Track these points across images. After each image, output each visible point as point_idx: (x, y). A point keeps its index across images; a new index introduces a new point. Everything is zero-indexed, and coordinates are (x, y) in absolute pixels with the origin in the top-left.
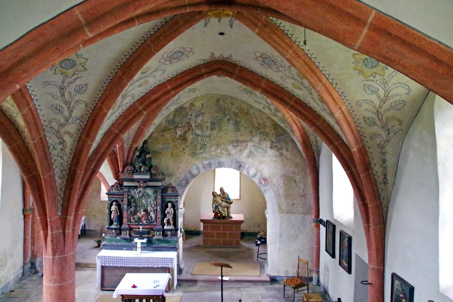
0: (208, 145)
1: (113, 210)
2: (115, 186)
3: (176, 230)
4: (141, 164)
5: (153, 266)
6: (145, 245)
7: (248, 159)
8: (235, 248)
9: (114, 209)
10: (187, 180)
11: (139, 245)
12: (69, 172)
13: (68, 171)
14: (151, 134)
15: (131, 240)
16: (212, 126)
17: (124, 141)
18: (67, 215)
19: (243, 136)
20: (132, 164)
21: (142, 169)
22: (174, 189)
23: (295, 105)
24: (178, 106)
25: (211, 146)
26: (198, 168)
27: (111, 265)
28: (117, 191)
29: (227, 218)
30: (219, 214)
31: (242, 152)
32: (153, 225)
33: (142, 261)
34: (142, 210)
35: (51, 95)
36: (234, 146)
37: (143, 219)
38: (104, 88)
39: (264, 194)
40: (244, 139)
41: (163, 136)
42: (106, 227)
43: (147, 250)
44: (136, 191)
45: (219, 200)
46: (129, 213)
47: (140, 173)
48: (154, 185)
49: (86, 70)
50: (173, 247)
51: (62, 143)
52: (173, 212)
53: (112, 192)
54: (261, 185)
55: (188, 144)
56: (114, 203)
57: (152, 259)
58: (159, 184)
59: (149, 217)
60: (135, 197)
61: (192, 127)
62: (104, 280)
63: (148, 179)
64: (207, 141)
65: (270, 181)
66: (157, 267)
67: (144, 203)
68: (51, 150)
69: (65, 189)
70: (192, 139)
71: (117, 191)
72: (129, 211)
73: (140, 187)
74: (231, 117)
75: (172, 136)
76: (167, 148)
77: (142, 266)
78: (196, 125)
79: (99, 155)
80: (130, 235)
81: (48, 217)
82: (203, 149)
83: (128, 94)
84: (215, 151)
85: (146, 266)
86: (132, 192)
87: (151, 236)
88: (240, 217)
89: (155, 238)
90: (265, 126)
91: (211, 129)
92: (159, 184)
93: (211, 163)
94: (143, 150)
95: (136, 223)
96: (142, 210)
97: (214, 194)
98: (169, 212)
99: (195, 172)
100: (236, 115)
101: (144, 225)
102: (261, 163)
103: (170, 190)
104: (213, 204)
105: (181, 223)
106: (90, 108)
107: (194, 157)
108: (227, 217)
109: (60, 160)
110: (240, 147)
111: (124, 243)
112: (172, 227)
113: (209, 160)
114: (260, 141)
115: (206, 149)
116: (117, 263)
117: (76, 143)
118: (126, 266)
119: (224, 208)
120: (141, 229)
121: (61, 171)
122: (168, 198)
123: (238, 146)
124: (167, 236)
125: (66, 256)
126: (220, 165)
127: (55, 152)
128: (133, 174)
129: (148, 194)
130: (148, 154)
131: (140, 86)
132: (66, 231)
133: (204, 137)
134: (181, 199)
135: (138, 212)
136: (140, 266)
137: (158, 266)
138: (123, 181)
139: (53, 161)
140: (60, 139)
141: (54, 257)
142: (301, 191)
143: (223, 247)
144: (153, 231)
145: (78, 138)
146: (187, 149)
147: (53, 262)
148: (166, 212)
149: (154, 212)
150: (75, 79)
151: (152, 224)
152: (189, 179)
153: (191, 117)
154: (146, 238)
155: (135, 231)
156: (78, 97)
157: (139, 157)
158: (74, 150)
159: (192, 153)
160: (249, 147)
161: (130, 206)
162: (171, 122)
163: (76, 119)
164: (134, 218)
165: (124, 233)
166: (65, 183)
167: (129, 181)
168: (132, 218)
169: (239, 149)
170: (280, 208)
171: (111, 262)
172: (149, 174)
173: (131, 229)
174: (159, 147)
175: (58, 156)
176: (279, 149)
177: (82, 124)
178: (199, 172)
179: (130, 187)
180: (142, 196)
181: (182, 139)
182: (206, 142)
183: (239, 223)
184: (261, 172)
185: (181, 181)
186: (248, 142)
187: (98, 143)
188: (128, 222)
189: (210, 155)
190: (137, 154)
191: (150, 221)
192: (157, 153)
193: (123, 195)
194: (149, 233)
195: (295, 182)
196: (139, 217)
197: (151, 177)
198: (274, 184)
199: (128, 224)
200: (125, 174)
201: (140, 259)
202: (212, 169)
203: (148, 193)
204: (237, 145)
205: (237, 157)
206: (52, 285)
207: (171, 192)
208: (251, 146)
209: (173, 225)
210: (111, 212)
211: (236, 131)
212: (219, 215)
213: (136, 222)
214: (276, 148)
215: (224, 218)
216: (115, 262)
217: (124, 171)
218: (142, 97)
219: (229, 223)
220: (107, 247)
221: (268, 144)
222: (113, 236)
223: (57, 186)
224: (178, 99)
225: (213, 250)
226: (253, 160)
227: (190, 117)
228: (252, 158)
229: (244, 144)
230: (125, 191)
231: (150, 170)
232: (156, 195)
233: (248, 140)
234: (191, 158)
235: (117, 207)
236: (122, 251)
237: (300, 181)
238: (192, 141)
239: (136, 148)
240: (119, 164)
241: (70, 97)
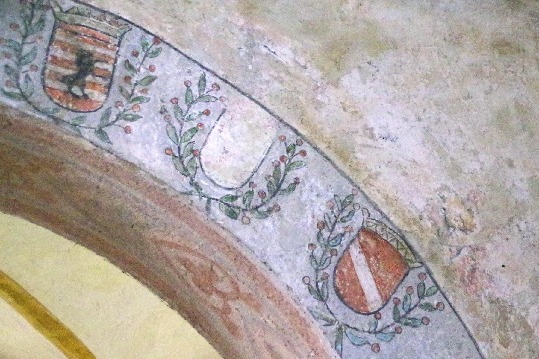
65: (448, 272)
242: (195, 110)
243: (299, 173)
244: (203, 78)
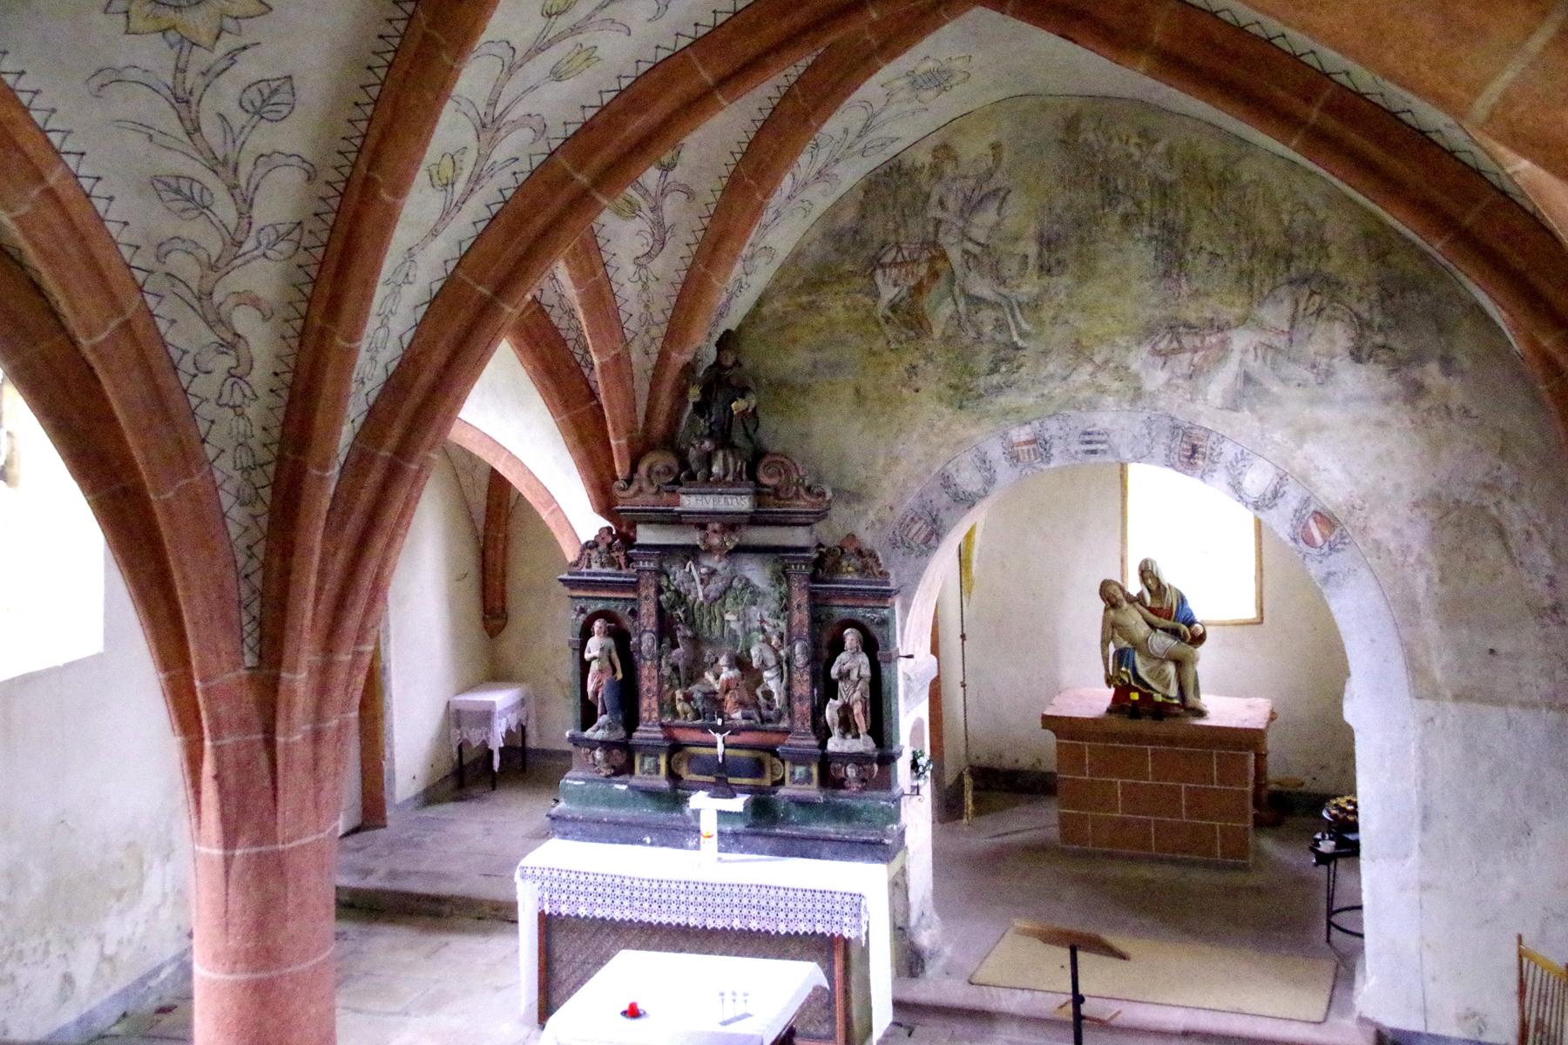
0: (1030, 346)
1: (595, 658)
2: (602, 547)
3: (887, 759)
4: (707, 444)
5: (771, 927)
6: (740, 827)
7: (1235, 414)
8: (1219, 867)
9: (596, 653)
10: (934, 521)
11: (709, 824)
12: (277, 471)
13: (271, 469)
14: (760, 303)
15: (675, 797)
16: (1046, 253)
17: (629, 336)
18: (278, 663)
19: (1203, 300)
20: (669, 442)
21: (716, 469)
22: (870, 561)
23: (1332, 124)
24: (876, 160)
25: (1045, 353)
26: (984, 462)
27: (582, 912)
29: (1177, 715)
30: (1136, 690)
31: (1201, 381)
32: (777, 731)
33: (718, 900)
34: (723, 661)
35: (144, 129)
36: (1156, 352)
37: (730, 700)
38: (375, 91)
39: (1326, 591)
40: (1208, 314)
41: (812, 307)
42: (567, 734)
43: (748, 849)
44: (697, 569)
45: (1135, 621)
46: (667, 671)
47: (710, 484)
48: (776, 543)
49: (271, 9)
50: (865, 842)
51: (233, 346)
52: (866, 672)
53: (589, 574)
54: (1305, 548)
55: (933, 343)
56: (597, 624)
57: (764, 891)
58: (798, 537)
59: (759, 692)
60: (690, 598)
61: (946, 260)
62: (554, 982)
63: (742, 513)
64: (1026, 327)
66: (788, 933)
67: (734, 626)
68: (185, 380)
69: (269, 552)
70: (952, 317)
71: (608, 570)
72: (663, 663)
73: (710, 551)
74: (1138, 204)
75: (856, 310)
76: (836, 367)
77: (720, 924)
78: (966, 252)
79: (415, 398)
80: (673, 776)
81: (196, 675)
82: (1003, 369)
83: (509, 117)
84: (1065, 379)
85: (737, 924)
86: (681, 574)
87: (767, 782)
88: (1247, 714)
89: (782, 791)
90: (1323, 244)
91: (1041, 267)
92: (798, 537)
93: (1047, 437)
94: (718, 377)
95: (699, 722)
96: (723, 661)
97: (1110, 595)
98: (849, 671)
99: (968, 479)
100: (1163, 191)
101: (736, 731)
102: (1301, 434)
103: (850, 569)
104: (1104, 644)
105: (917, 729)
106: (328, 183)
107: (960, 408)
108: (1176, 710)
109: (234, 423)
110: (1188, 355)
111: (647, 811)
112: (863, 744)
113: (1036, 424)
114: (1293, 320)
115: (1019, 367)
116: (608, 901)
117: (295, 343)
118: (645, 917)
119: (1163, 661)
120: (720, 749)
121: (244, 470)
122: (840, 602)
123: (1181, 349)
124: (844, 787)
125: (280, 847)
126: (1093, 447)
127: (203, 387)
128: (674, 492)
129: (747, 583)
130: (743, 396)
131: (557, 75)
132: (280, 739)
133: (1007, 310)
134: (906, 608)
135: (705, 667)
136: (710, 924)
137: (791, 925)
138: (632, 526)
139: (203, 427)
140: (220, 329)
141: (230, 853)
142: (1539, 586)
143: (1161, 861)
144: (776, 761)
145: (299, 323)
146: (930, 367)
147: (227, 873)
148: (834, 672)
149: (782, 668)
150: (232, 56)
151: (770, 726)
153: (938, 213)
154: (744, 792)
155: (692, 757)
156: (264, 138)
157: (700, 409)
158: (288, 378)
159: (951, 386)
160: (1235, 357)
161: (667, 640)
162: (847, 238)
163: (273, 237)
164: (688, 698)
165: (646, 767)
166: (263, 521)
167: (662, 523)
168: (679, 694)
169: (1186, 363)
170: (1416, 670)
171: (582, 899)
172: (748, 490)
173: (675, 747)
174: (797, 360)
175: (222, 401)
176: (1397, 366)
177: (302, 257)
178: (990, 482)
179: (666, 551)
180: (723, 594)
181: (905, 323)
183: (1244, 741)
184: (1304, 479)
185: (905, 525)
187: (405, 346)
188: (662, 713)
189: (1043, 395)
190: (694, 394)
191: (762, 714)
192: (783, 390)
193: (634, 586)
194: (757, 769)
195: (1501, 533)
196: (711, 693)
197: (759, 506)
198: (1378, 544)
199: (662, 725)
200: (640, 490)
201: (709, 889)
202: (1052, 465)
203: (747, 580)
204: (1175, 345)
205: (1177, 405)
206: (223, 976)
207: (856, 577)
208: (1244, 352)
209: (869, 733)
210: (585, 666)
211: (1166, 274)
212: (1135, 696)
213: (698, 715)
214: (1384, 357)
215: (1161, 711)
216: (600, 900)
217: (636, 476)
218: (585, 124)
219: (1184, 741)
220: (569, 827)
221: (1341, 336)
222: (595, 776)
223: (233, 537)
224: (866, 127)
225: (1115, 870)
226: (1261, 419)
227: (935, 212)
228: (1252, 410)
229: (1214, 339)
230: (644, 570)
231: (752, 474)
232: (784, 588)
233: (1233, 323)
234: (947, 411)
235: (610, 642)
236: (638, 848)
237: (1528, 533)
238: (949, 332)
239: (689, 369)
240: (613, 442)
241: (229, 137)
242: (1240, 465)
243: (1285, 488)
244: (1242, 452)
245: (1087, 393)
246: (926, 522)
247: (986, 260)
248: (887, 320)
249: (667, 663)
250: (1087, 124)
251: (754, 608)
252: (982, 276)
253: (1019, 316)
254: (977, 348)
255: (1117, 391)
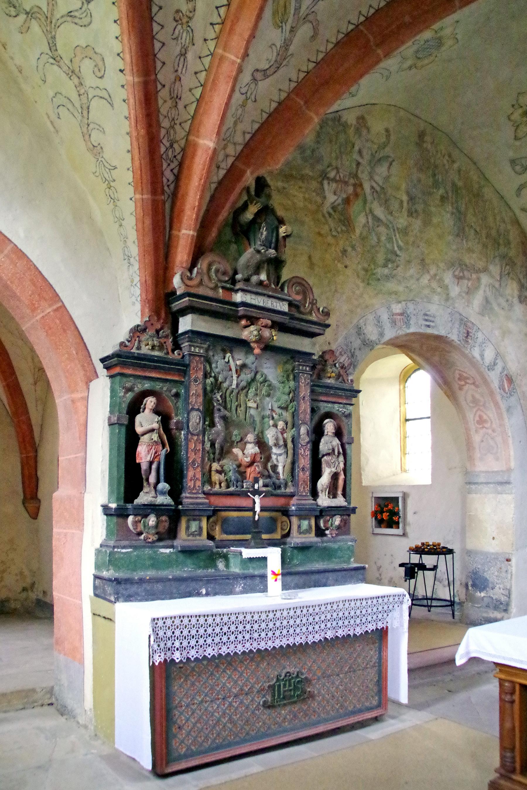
10: (353, 356)
28: (156, 353)
36: (455, 276)
46: (208, 445)
60: (225, 385)
61: (363, 189)
67: (252, 412)
70: (364, 226)
75: (311, 202)
82: (390, 266)
84: (418, 280)
103: (333, 374)
115: (397, 267)
135: (232, 444)
146: (353, 254)
152: (357, 353)
180: (249, 384)
181: (340, 221)
182: (397, 247)
186: (480, 272)
188: (203, 484)
205: (460, 306)
226: (492, 322)
234: (362, 285)
238: (365, 233)
245: (426, 291)
246: (348, 356)
247: (382, 196)
248: (330, 214)
249: (208, 438)
250: (428, 138)
251: (267, 399)
252: (381, 205)
253: (398, 235)
254: (377, 249)
255: (439, 294)
